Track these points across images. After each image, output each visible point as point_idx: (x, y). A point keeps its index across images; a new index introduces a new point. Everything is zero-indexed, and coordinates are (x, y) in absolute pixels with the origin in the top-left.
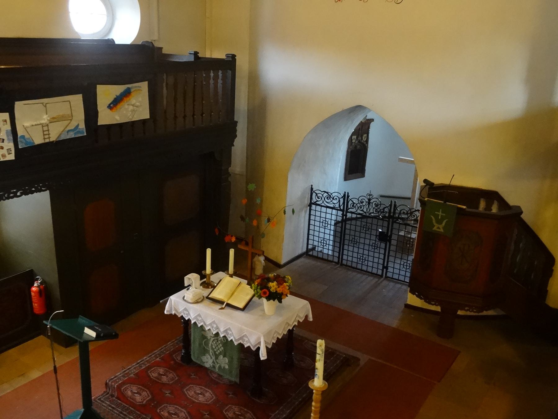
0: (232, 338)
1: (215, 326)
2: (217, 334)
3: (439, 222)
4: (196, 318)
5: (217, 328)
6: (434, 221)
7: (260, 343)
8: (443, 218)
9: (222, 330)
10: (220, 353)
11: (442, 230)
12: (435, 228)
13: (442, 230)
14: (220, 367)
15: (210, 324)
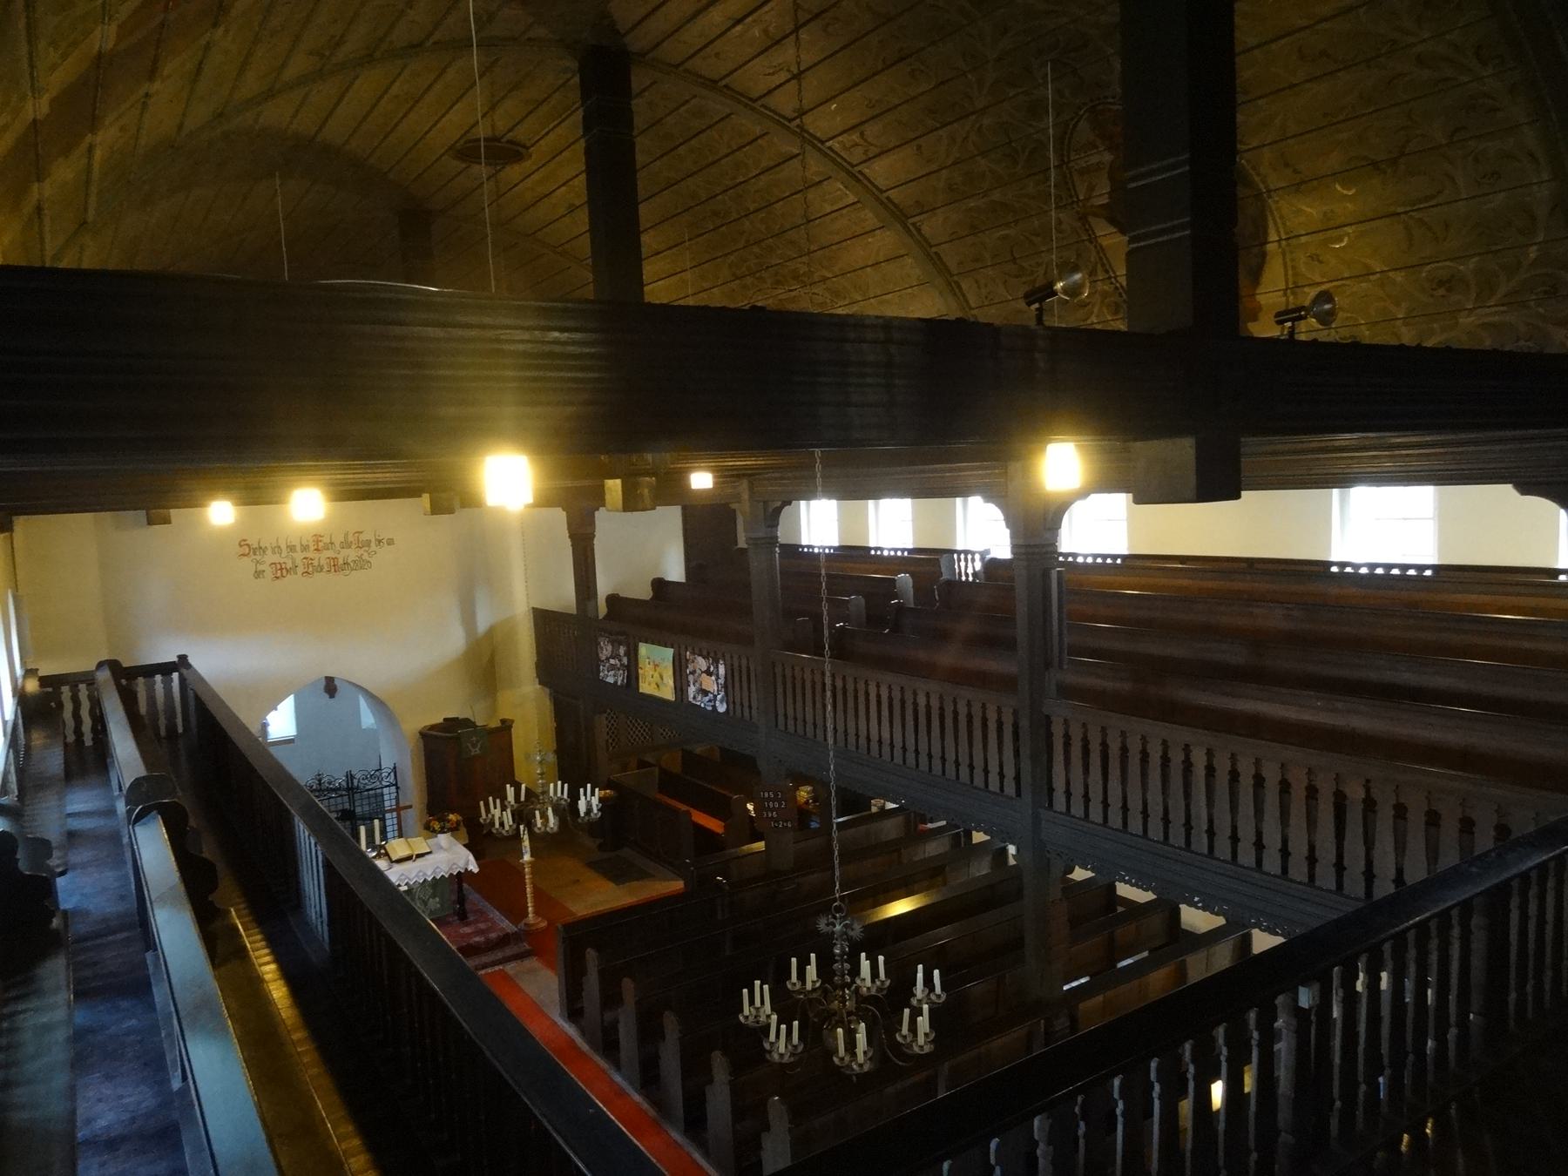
0: (442, 873)
1: (421, 874)
2: (425, 880)
3: (474, 746)
4: (399, 879)
5: (425, 874)
6: (471, 748)
7: (467, 863)
8: (478, 741)
9: (429, 873)
10: (428, 899)
11: (478, 752)
12: (473, 754)
13: (478, 752)
14: (431, 911)
15: (416, 876)
